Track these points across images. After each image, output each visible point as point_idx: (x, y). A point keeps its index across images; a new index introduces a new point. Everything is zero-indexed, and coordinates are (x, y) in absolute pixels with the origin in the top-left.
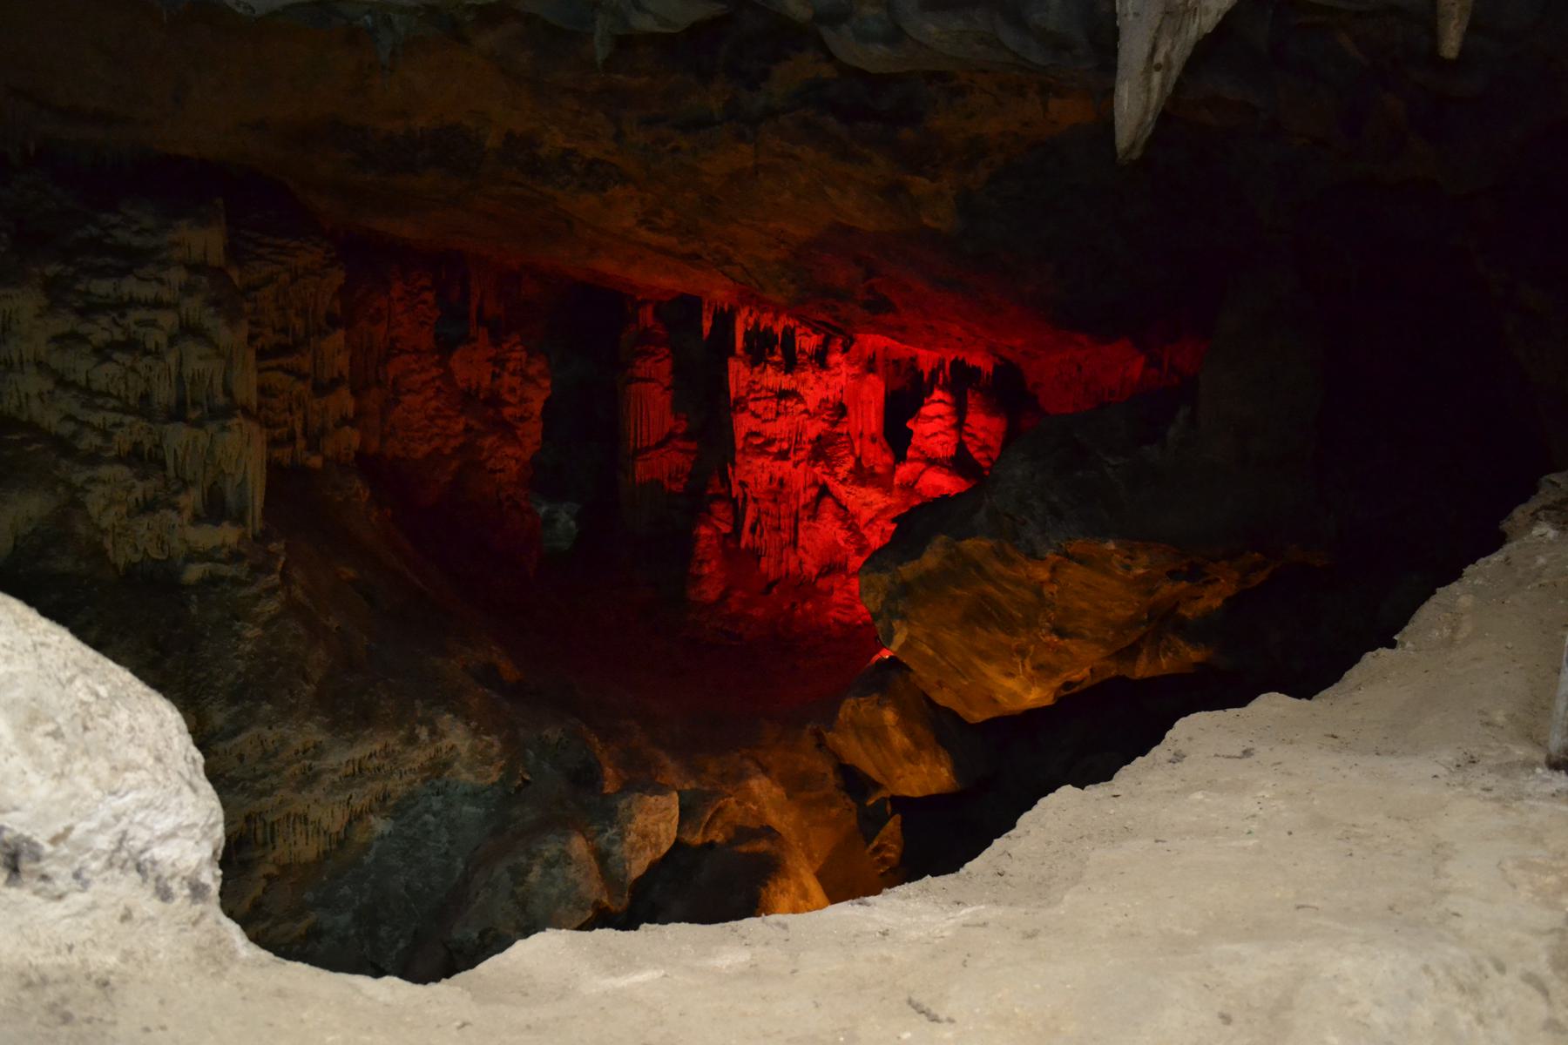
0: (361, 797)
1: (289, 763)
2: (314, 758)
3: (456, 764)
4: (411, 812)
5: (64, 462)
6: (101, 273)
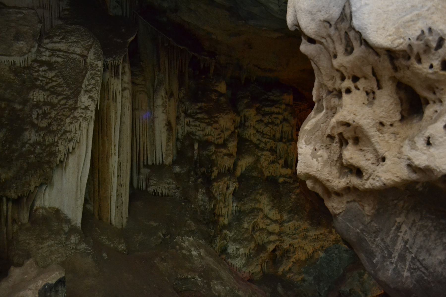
0: (318, 245)
1: (301, 232)
4: (330, 252)
5: (257, 150)
6: (267, 106)
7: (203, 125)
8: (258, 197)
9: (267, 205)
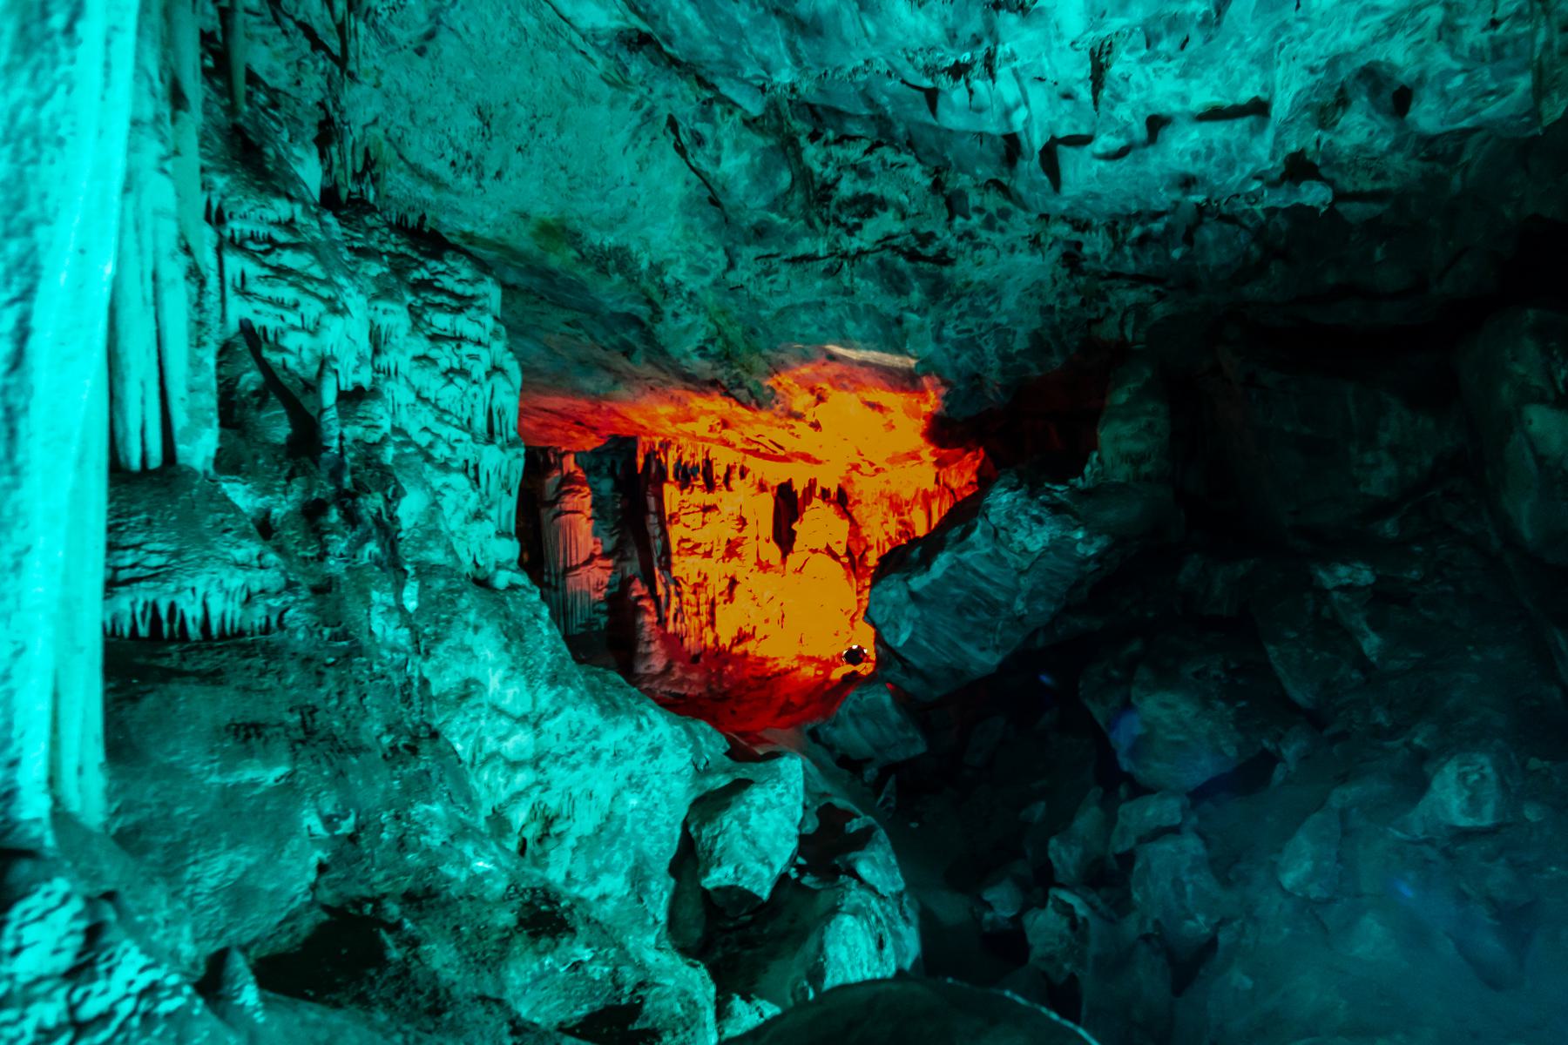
2: (597, 738)
5: (428, 467)
7: (312, 308)
9: (495, 666)
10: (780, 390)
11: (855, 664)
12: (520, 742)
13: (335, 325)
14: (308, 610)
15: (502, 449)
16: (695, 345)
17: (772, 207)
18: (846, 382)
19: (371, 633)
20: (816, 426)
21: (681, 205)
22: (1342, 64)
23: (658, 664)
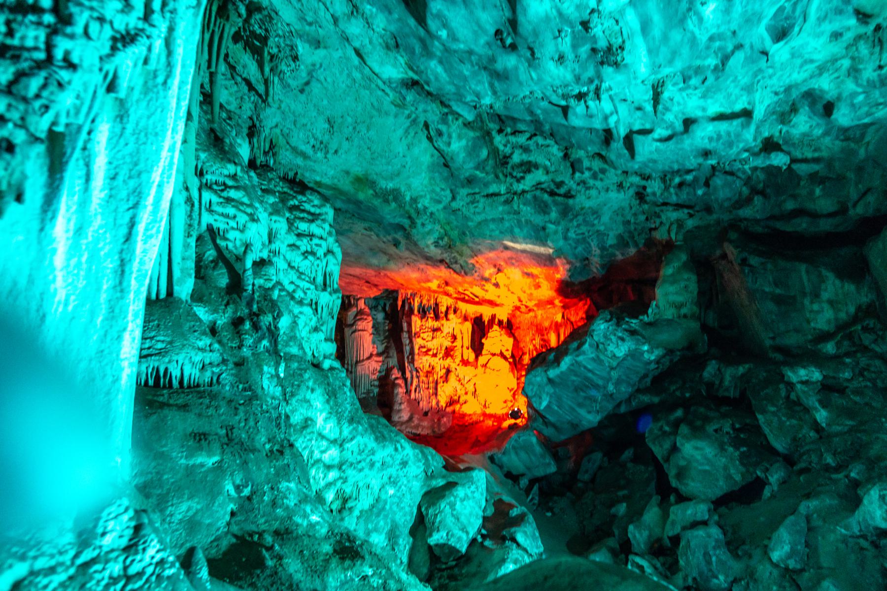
2: (373, 454)
3: (410, 463)
4: (399, 484)
5: (292, 303)
8: (309, 395)
9: (321, 411)
10: (477, 266)
11: (516, 419)
12: (332, 455)
13: (253, 228)
14: (232, 375)
15: (330, 294)
16: (432, 241)
17: (477, 168)
18: (514, 261)
19: (262, 388)
20: (497, 285)
21: (428, 167)
22: (793, 90)
23: (405, 416)
